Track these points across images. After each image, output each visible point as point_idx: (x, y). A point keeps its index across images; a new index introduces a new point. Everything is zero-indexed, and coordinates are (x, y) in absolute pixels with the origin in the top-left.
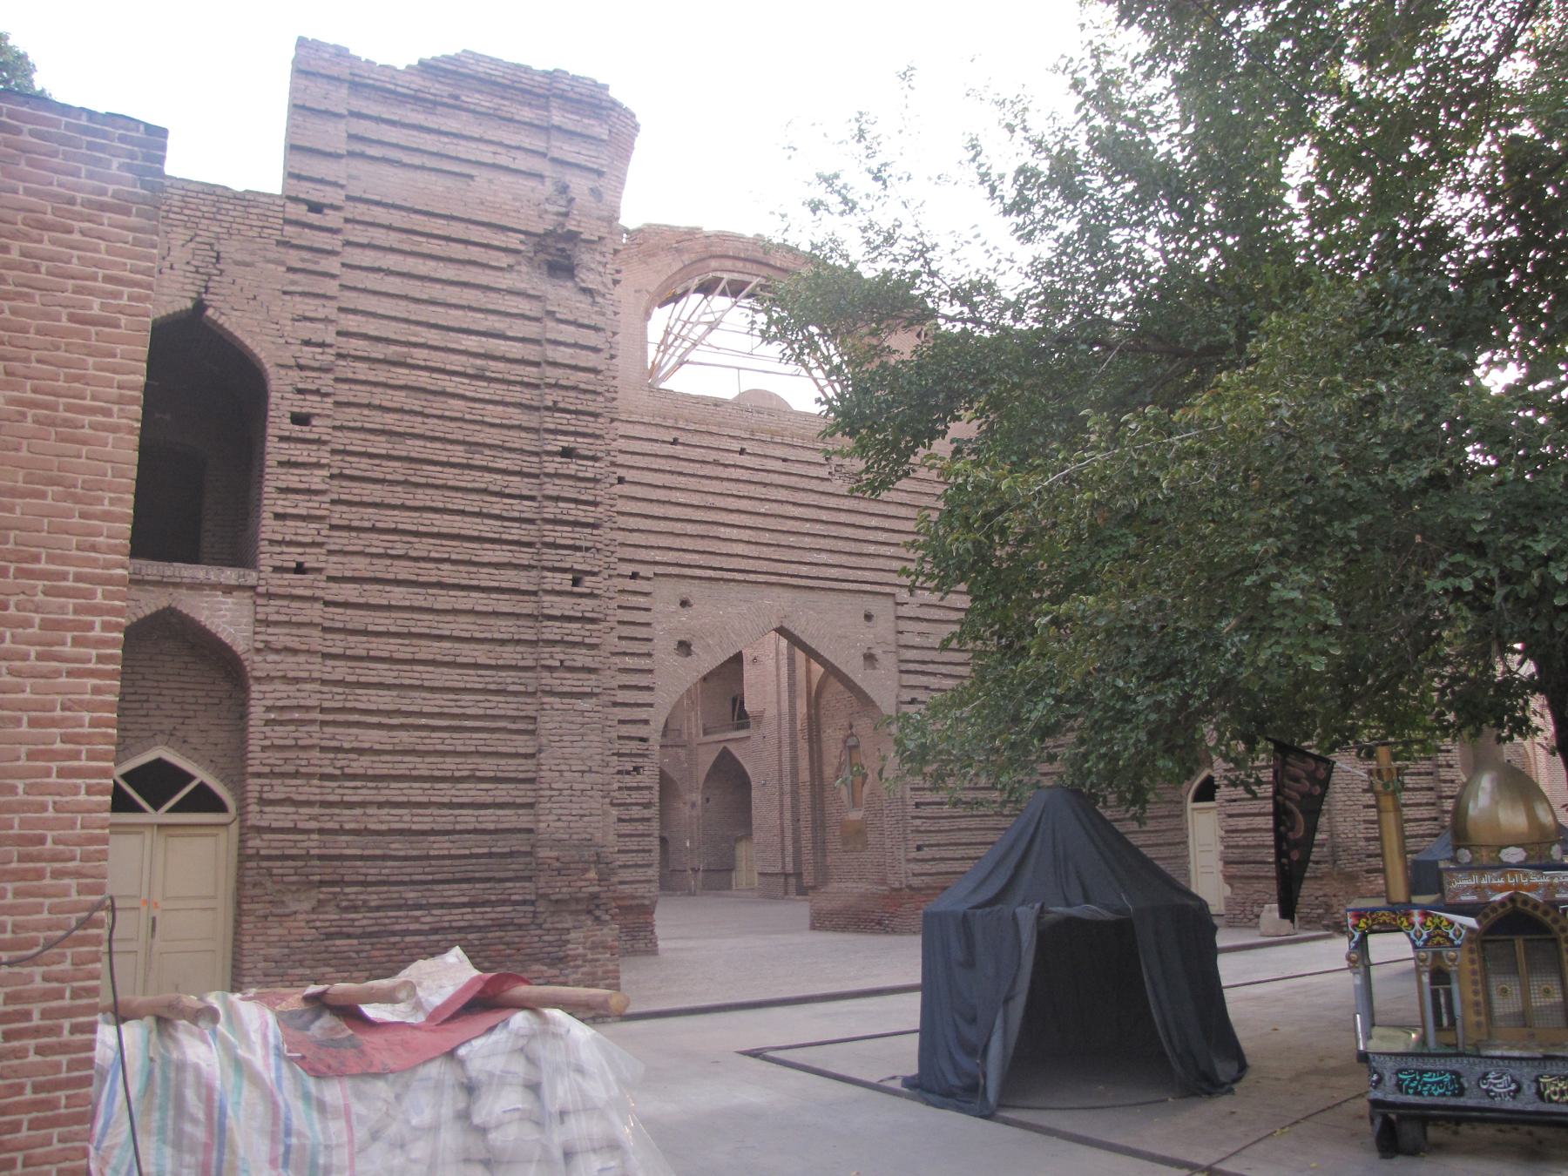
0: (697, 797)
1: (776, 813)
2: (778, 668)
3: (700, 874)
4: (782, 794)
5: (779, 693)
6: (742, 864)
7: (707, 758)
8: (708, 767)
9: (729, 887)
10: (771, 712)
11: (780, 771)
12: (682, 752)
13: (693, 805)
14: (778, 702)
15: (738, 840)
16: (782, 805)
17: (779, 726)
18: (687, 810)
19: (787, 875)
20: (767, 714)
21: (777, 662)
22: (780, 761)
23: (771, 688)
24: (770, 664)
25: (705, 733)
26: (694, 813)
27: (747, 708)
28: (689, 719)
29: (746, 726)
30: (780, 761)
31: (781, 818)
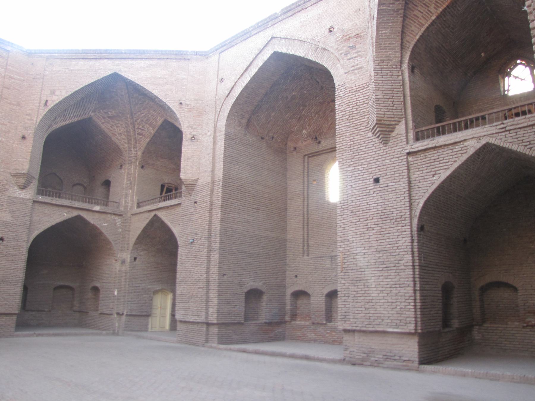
0: (127, 256)
1: (203, 269)
2: (215, 143)
3: (124, 318)
4: (210, 251)
5: (213, 164)
6: (157, 311)
7: (139, 225)
8: (139, 232)
9: (146, 330)
10: (205, 179)
11: (210, 229)
12: (118, 220)
13: (123, 262)
14: (213, 171)
15: (156, 292)
16: (209, 261)
17: (212, 191)
18: (117, 266)
19: (208, 324)
20: (200, 182)
21: (215, 138)
22: (210, 221)
23: (206, 160)
24: (207, 140)
25: (138, 207)
26: (124, 269)
27: (182, 176)
28: (127, 195)
30: (210, 221)
31: (208, 273)
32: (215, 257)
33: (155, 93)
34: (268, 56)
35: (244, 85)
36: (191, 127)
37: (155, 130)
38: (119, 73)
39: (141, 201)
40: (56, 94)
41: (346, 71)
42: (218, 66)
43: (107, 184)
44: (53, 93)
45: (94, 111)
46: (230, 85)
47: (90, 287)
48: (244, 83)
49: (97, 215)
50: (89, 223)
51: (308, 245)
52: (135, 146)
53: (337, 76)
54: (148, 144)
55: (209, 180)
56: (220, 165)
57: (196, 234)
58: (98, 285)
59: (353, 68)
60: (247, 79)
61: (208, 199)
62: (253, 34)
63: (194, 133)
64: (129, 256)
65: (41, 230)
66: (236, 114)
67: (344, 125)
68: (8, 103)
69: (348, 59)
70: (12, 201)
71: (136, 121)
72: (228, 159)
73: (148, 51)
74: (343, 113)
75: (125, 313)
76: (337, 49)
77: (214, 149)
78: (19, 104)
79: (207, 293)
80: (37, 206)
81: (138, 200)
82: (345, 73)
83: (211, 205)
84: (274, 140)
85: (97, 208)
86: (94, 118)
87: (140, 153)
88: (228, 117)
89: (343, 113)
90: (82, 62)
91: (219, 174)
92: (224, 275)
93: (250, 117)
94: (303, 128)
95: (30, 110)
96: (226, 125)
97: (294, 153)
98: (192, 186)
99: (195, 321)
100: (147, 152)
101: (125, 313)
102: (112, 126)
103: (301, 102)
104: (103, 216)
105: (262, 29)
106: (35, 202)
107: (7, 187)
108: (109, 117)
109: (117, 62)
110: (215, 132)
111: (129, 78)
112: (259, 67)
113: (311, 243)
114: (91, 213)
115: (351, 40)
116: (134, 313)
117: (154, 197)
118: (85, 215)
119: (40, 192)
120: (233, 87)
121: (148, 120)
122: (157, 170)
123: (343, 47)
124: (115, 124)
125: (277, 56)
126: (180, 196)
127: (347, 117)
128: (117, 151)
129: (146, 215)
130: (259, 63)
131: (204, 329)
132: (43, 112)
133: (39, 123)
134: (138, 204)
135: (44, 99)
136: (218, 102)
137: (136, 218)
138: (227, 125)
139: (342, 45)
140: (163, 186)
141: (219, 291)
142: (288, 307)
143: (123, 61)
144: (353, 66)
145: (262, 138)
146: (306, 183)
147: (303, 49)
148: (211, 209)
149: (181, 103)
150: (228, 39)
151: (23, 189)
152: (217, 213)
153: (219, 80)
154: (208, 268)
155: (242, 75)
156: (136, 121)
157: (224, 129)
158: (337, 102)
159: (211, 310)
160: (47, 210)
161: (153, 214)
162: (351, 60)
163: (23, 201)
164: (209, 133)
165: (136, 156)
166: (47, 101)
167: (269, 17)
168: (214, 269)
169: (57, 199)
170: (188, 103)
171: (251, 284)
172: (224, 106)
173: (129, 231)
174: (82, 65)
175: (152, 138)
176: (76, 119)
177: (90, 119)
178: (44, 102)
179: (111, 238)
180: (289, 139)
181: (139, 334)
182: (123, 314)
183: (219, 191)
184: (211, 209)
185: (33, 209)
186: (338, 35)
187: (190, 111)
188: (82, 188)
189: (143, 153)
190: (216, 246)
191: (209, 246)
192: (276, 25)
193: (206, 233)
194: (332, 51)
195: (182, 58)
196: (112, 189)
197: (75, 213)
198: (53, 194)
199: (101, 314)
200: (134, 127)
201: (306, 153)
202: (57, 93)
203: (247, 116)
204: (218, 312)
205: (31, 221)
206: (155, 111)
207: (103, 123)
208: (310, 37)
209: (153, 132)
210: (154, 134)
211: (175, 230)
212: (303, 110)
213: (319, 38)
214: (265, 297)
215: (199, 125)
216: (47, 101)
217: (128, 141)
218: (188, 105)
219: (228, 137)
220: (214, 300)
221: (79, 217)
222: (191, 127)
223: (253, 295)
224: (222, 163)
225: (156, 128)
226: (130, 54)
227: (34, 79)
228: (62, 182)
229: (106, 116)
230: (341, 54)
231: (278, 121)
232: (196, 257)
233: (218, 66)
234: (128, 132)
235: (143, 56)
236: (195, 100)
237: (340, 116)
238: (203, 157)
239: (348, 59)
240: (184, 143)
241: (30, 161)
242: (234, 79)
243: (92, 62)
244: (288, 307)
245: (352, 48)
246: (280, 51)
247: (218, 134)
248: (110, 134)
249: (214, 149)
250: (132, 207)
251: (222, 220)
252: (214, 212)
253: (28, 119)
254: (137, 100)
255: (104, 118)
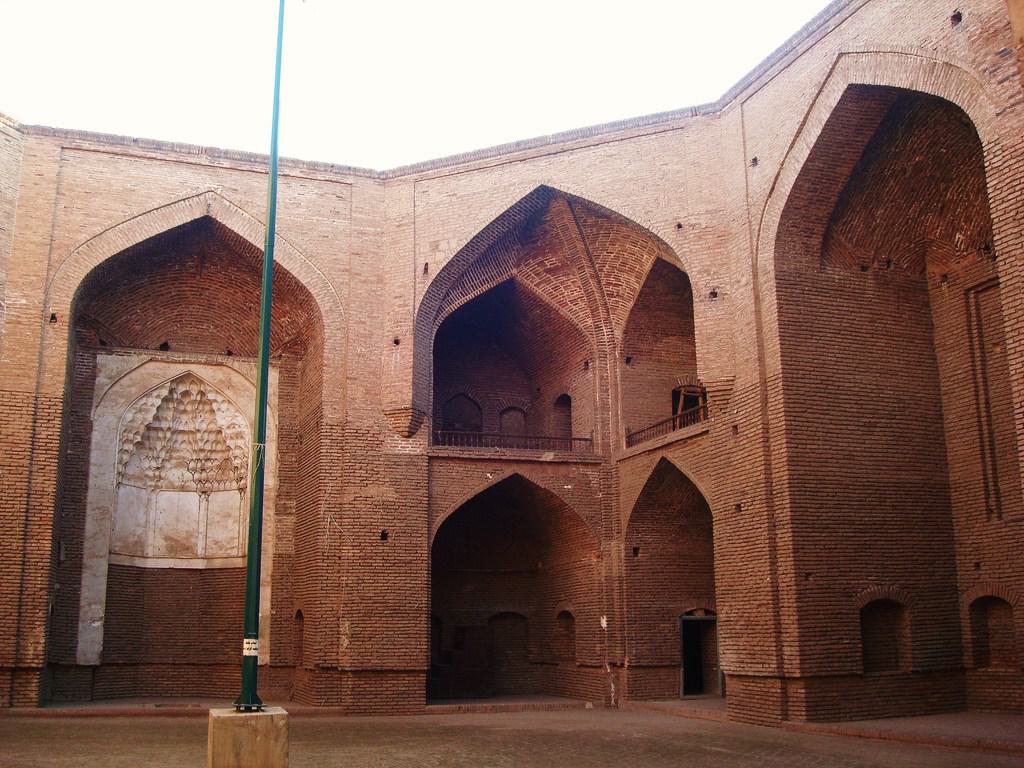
0: (617, 548)
2: (757, 299)
3: (624, 672)
4: (773, 527)
7: (632, 481)
12: (593, 475)
14: (761, 359)
16: (774, 548)
17: (765, 401)
20: (739, 385)
22: (768, 465)
23: (745, 336)
24: (740, 294)
25: (629, 444)
29: (693, 418)
30: (768, 465)
31: (774, 572)
32: (785, 537)
33: (625, 213)
34: (839, 98)
35: (799, 167)
36: (705, 271)
37: (642, 283)
38: (549, 185)
39: (633, 431)
40: (440, 248)
41: (998, 111)
42: (743, 133)
43: (565, 402)
44: (435, 247)
45: (517, 265)
46: (768, 169)
47: (557, 611)
48: (798, 162)
49: (550, 469)
50: (538, 488)
51: (997, 491)
52: (607, 321)
53: (983, 123)
54: (632, 311)
55: (755, 377)
56: (773, 345)
57: (744, 493)
58: (570, 608)
59: (1012, 101)
60: (802, 153)
61: (757, 419)
62: (800, 51)
63: (714, 283)
64: (623, 546)
65: (450, 511)
66: (795, 230)
67: (1009, 232)
68: (364, 282)
69: (1000, 82)
70: (394, 462)
71: (601, 270)
72: (793, 328)
73: (596, 128)
74: (1004, 205)
75: (626, 664)
76: (974, 61)
77: (758, 312)
78: (380, 280)
79: (777, 615)
80: (436, 463)
81: (628, 430)
82: (998, 115)
83: (766, 430)
84: (892, 268)
85: (549, 456)
86: (519, 278)
87: (618, 333)
88: (778, 239)
89: (1004, 205)
90: (477, 177)
91: (775, 364)
92: (808, 575)
93: (828, 229)
94: (956, 229)
95: (400, 286)
96: (776, 259)
97: (944, 286)
98: (726, 391)
99: (757, 674)
100: (632, 328)
101: (626, 664)
102: (556, 288)
103: (938, 174)
104: (562, 470)
105: (818, 37)
106: (431, 458)
107: (381, 438)
108: (548, 271)
109: (542, 163)
110: (755, 276)
111: (570, 192)
112: (824, 123)
113: (1003, 487)
114: (538, 468)
115: (1000, 37)
116: (644, 662)
117: (660, 420)
118: (524, 471)
119: (436, 441)
120: (778, 174)
121: (624, 264)
122: (659, 361)
123: (986, 55)
124: (562, 283)
125: (857, 93)
126: (706, 417)
127: (1012, 213)
128: (574, 333)
129: (646, 460)
130: (823, 114)
131: (776, 688)
132: (423, 289)
133: (420, 310)
134: (629, 437)
135: (421, 262)
136: (753, 210)
137: (624, 469)
138: (779, 258)
139: (983, 51)
140: (676, 394)
141: (799, 610)
142: (968, 636)
143: (552, 159)
144: (1011, 97)
145: (864, 269)
146: (978, 353)
147: (906, 72)
148: (766, 440)
149: (680, 226)
150: (754, 71)
151: (409, 437)
152: (780, 447)
153: (749, 163)
154: (773, 564)
155: (791, 147)
156: (601, 270)
157: (773, 267)
158: (991, 182)
159: (787, 651)
160: (457, 469)
161: (657, 457)
162: (1006, 84)
163: (411, 460)
164: (744, 281)
165: (612, 341)
166: (427, 264)
167: (827, 11)
168: (786, 565)
169: (472, 448)
170: (693, 221)
171: (871, 589)
172: (767, 217)
173: (618, 495)
174: (479, 182)
175: (638, 300)
176: (486, 288)
177: (512, 281)
178: (421, 268)
179: (583, 512)
180: (928, 258)
181: (656, 703)
182: (622, 665)
183: (777, 400)
184: (766, 440)
185: (430, 473)
186: (971, 29)
187: (700, 238)
188: (520, 416)
189: (625, 332)
190: (784, 514)
191: (771, 516)
192: (843, 25)
193: (762, 490)
194: (965, 67)
195: (667, 128)
196: (574, 414)
197: (508, 471)
198: (462, 439)
199: (581, 666)
200: (599, 282)
201: (971, 285)
202: (443, 245)
203: (820, 229)
204: (802, 653)
205: (430, 497)
206: (635, 244)
207: (537, 285)
208: (916, 43)
209: (638, 287)
210: (641, 292)
211: (705, 487)
212: (946, 189)
213: (935, 41)
214: (907, 616)
215: (723, 265)
216: (427, 264)
217: (592, 311)
218: (693, 226)
219: (783, 282)
220: (792, 630)
221: (515, 477)
222: (708, 272)
223: (879, 613)
224: (777, 341)
225: (644, 278)
226: (563, 141)
227: (399, 226)
228: (480, 409)
229: (541, 270)
230: (985, 71)
231: (893, 224)
232: (747, 540)
233: (743, 133)
234: (589, 294)
235: (591, 140)
236: (707, 212)
237: (999, 213)
238: (737, 331)
239: (1000, 82)
240: (699, 307)
241: (414, 383)
242: (778, 156)
243: (498, 172)
244: (968, 636)
245: (1004, 54)
246: (859, 82)
247: (762, 279)
248: (554, 304)
249: (758, 312)
250: (618, 447)
251: (791, 461)
252: (773, 443)
253: (400, 306)
254: (594, 229)
255: (537, 275)
